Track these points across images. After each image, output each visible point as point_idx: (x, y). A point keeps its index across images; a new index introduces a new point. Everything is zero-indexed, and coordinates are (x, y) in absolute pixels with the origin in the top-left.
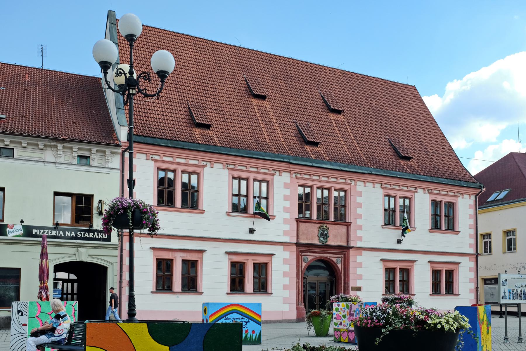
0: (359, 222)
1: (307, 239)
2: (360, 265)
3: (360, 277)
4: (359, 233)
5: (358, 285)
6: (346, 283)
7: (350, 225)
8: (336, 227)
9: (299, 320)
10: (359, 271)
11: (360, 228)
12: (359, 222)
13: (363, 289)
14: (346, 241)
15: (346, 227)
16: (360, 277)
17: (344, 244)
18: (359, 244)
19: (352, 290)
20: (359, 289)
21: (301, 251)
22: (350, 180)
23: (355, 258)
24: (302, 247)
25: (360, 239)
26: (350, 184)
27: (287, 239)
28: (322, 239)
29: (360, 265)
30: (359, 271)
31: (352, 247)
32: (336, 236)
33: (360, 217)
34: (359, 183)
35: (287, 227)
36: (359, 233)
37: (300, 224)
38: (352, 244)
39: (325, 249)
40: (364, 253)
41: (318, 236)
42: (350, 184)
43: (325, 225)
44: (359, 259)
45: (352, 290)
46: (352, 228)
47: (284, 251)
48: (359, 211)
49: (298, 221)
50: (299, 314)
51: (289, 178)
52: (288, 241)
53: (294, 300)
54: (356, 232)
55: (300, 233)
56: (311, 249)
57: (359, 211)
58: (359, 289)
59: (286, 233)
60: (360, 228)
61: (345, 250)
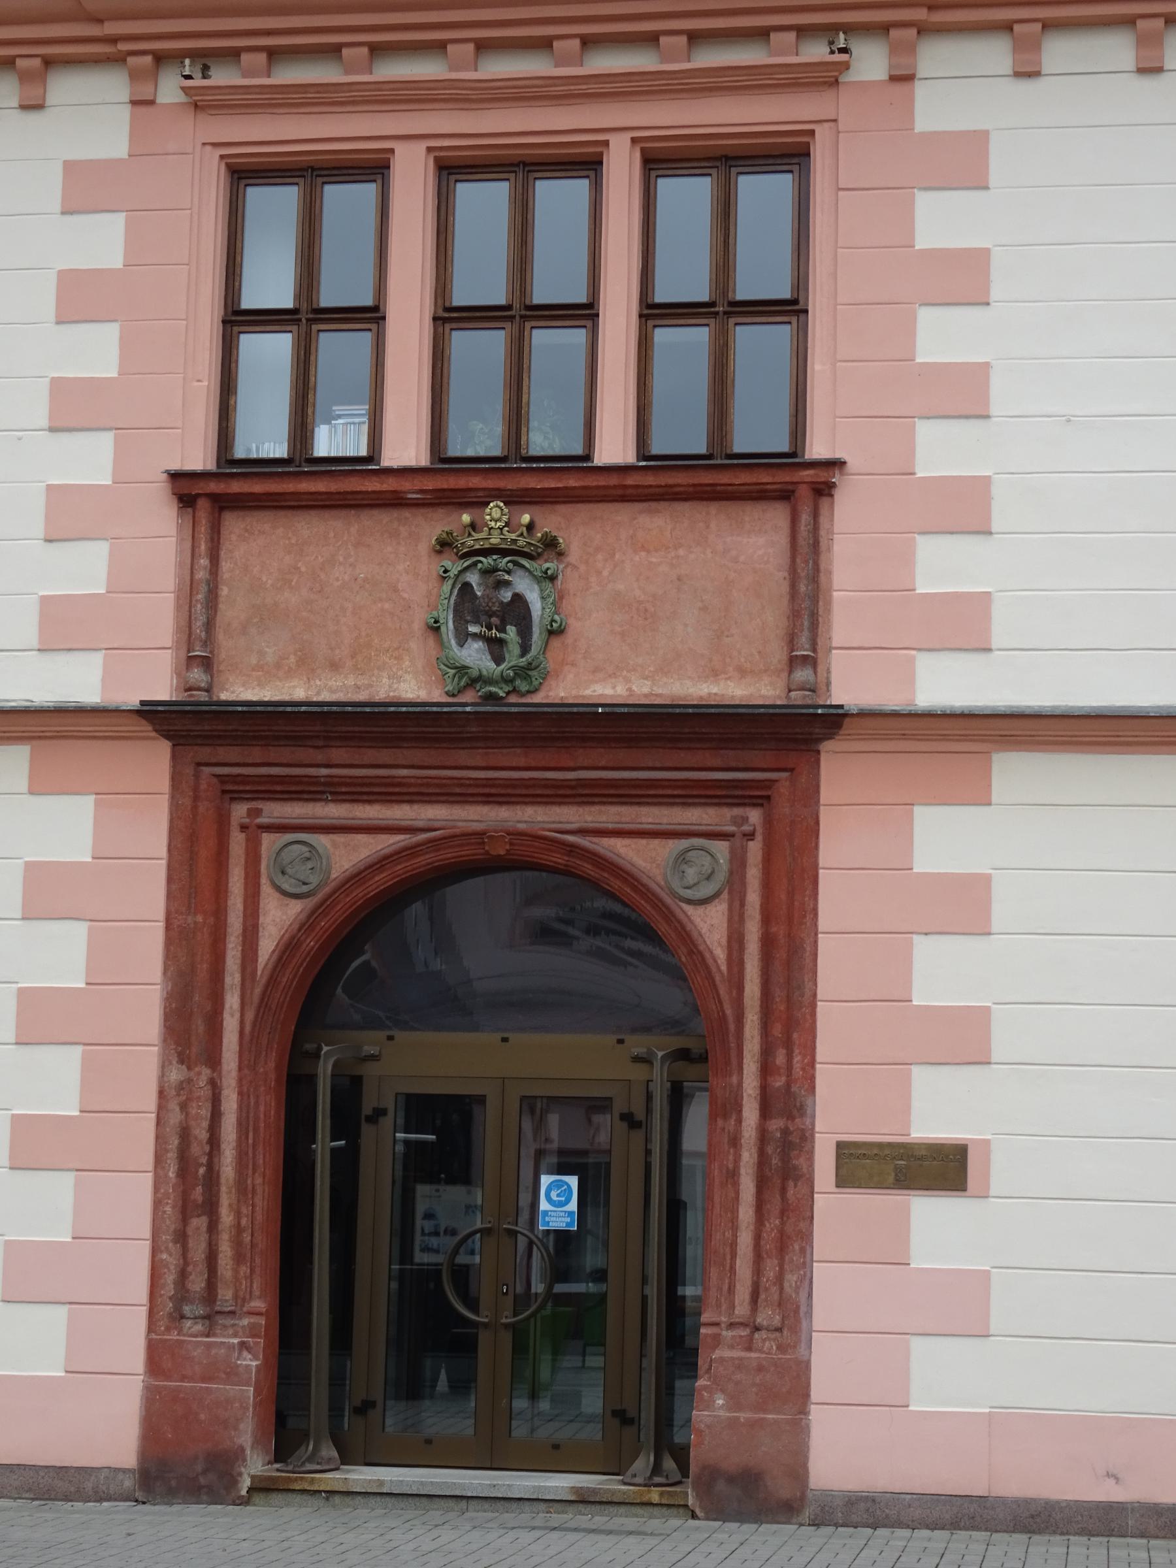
0: (941, 450)
1: (305, 664)
2: (964, 905)
3: (963, 1039)
4: (942, 566)
5: (928, 1127)
6: (787, 1103)
7: (824, 490)
8: (656, 523)
9: (176, 1468)
10: (942, 972)
11: (965, 508)
12: (941, 450)
13: (1003, 1170)
14: (777, 654)
15: (776, 516)
16: (963, 1039)
17: (761, 690)
18: (944, 683)
19: (843, 1181)
20: (943, 1169)
21: (233, 789)
22: (831, 30)
23: (884, 846)
24: (224, 752)
25: (964, 624)
26: (828, 78)
27: (79, 681)
28: (474, 655)
29: (964, 905)
30: (942, 972)
31: (834, 721)
32: (643, 622)
33: (964, 393)
34: (937, 58)
35: (85, 569)
36: (942, 566)
37: (234, 525)
38: (849, 687)
39: (517, 756)
40: (1015, 773)
41: (435, 628)
42: (828, 78)
43: (495, 511)
44: (944, 838)
45: (843, 1181)
46: (849, 518)
47: (34, 790)
48: (942, 336)
49: (219, 495)
50: (164, 1418)
51: (125, 112)
52: (90, 694)
53: (128, 1271)
54: (907, 559)
55: (232, 611)
56: (342, 761)
57: (942, 336)
58: (943, 1169)
59: (62, 624)
60: (965, 508)
61: (766, 754)
